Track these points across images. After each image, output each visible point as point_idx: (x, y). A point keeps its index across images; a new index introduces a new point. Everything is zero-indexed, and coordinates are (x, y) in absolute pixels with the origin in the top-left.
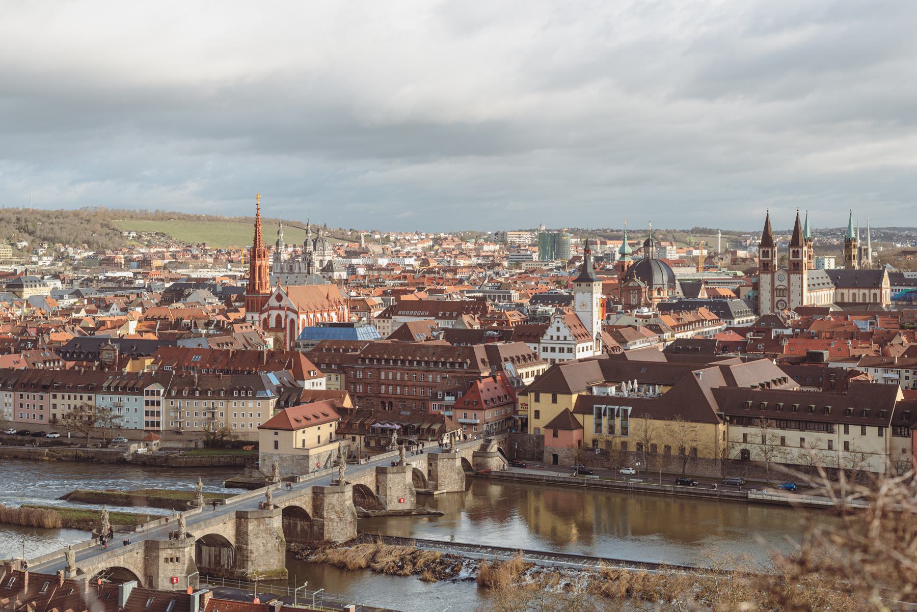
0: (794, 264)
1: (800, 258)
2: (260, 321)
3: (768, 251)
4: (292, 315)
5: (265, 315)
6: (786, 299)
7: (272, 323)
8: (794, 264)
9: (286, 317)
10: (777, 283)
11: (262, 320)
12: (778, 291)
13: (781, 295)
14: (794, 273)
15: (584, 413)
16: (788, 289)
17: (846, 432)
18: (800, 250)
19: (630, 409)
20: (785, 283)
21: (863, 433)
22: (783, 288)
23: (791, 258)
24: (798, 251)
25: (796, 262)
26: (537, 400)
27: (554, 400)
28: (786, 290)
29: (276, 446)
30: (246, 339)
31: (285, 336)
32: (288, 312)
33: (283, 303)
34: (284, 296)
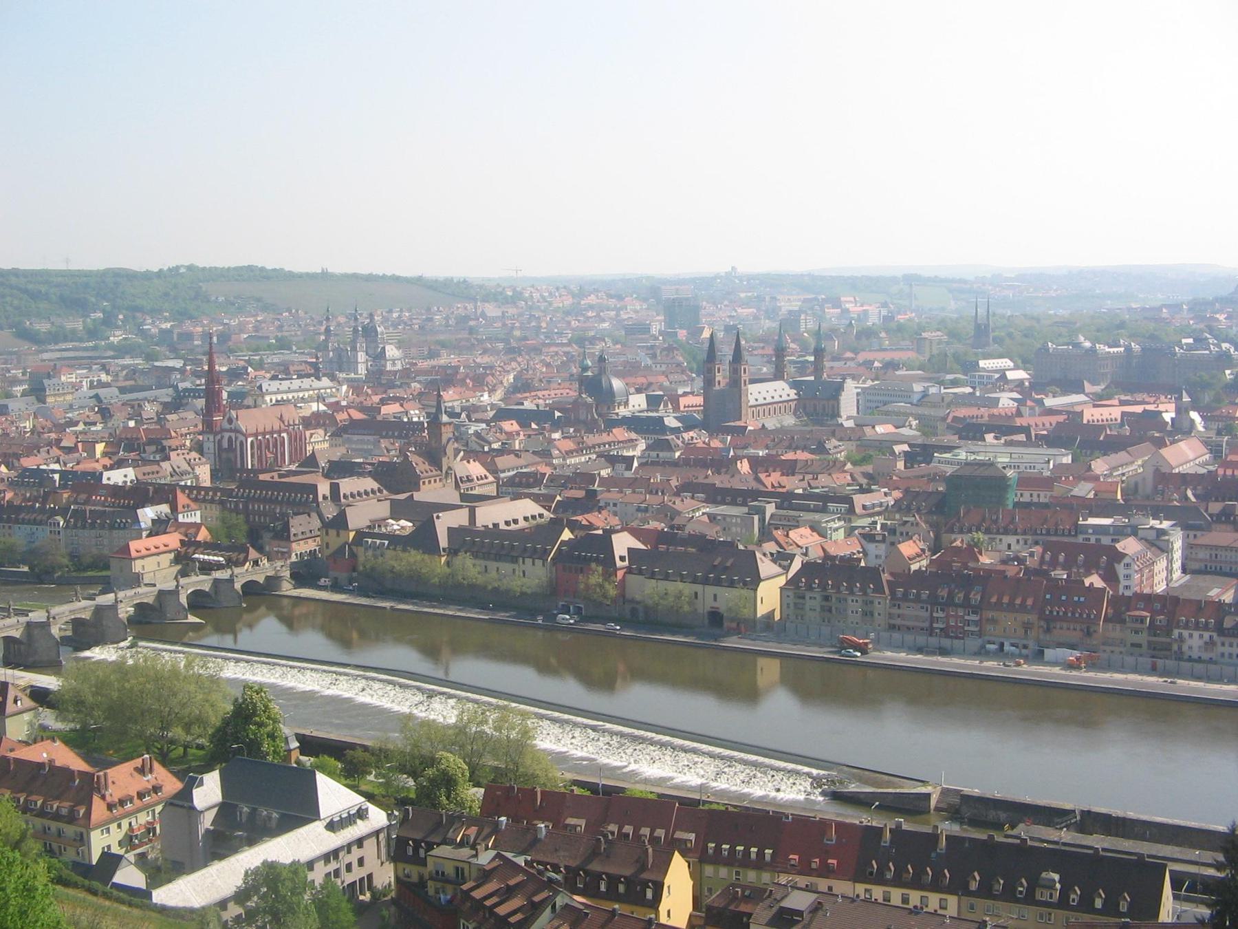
2: (214, 442)
4: (241, 438)
5: (219, 437)
7: (225, 444)
9: (236, 438)
11: (217, 441)
15: (357, 546)
17: (524, 563)
19: (386, 542)
21: (533, 564)
26: (327, 534)
27: (338, 535)
29: (121, 571)
30: (173, 469)
31: (236, 457)
32: (238, 435)
33: (233, 426)
34: (234, 421)
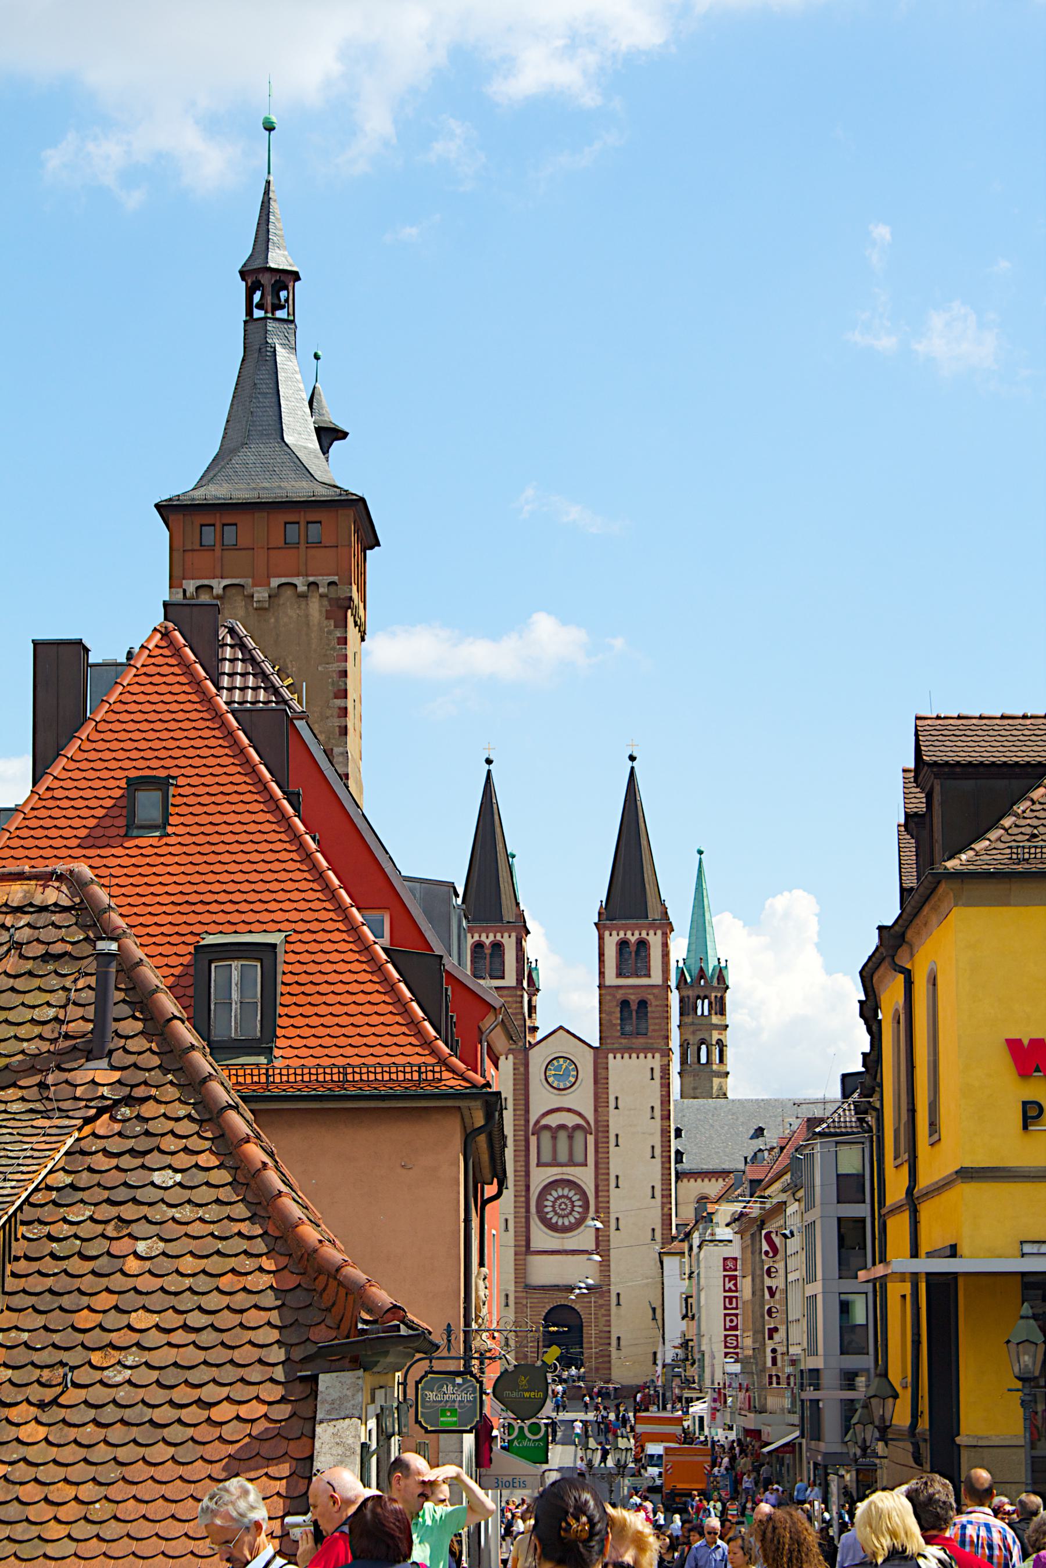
0: (625, 1004)
1: (656, 978)
3: (498, 946)
6: (585, 1177)
8: (625, 1004)
10: (542, 1099)
12: (546, 1136)
13: (563, 1156)
14: (629, 1050)
16: (601, 1129)
18: (655, 940)
20: (582, 1098)
22: (571, 1120)
23: (611, 979)
24: (643, 944)
25: (633, 998)
28: (587, 1131)
